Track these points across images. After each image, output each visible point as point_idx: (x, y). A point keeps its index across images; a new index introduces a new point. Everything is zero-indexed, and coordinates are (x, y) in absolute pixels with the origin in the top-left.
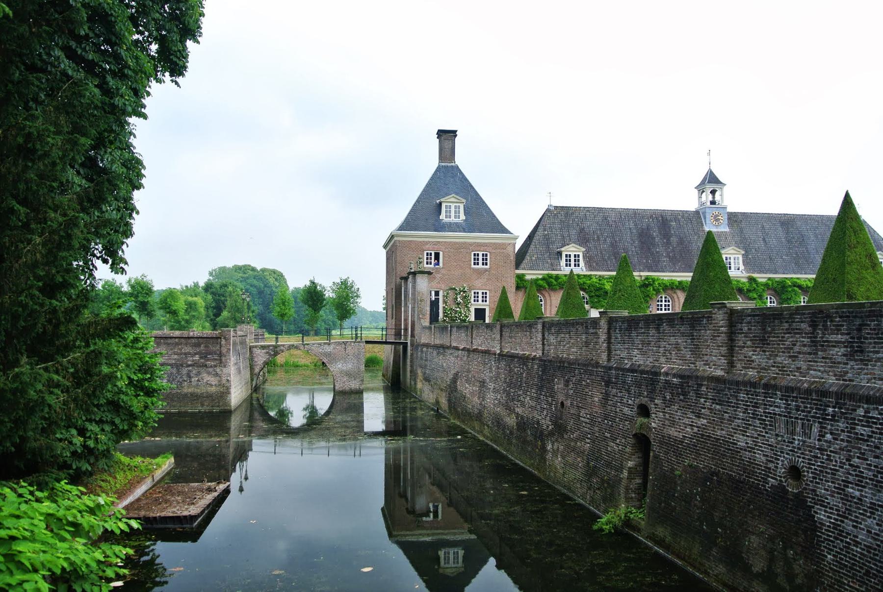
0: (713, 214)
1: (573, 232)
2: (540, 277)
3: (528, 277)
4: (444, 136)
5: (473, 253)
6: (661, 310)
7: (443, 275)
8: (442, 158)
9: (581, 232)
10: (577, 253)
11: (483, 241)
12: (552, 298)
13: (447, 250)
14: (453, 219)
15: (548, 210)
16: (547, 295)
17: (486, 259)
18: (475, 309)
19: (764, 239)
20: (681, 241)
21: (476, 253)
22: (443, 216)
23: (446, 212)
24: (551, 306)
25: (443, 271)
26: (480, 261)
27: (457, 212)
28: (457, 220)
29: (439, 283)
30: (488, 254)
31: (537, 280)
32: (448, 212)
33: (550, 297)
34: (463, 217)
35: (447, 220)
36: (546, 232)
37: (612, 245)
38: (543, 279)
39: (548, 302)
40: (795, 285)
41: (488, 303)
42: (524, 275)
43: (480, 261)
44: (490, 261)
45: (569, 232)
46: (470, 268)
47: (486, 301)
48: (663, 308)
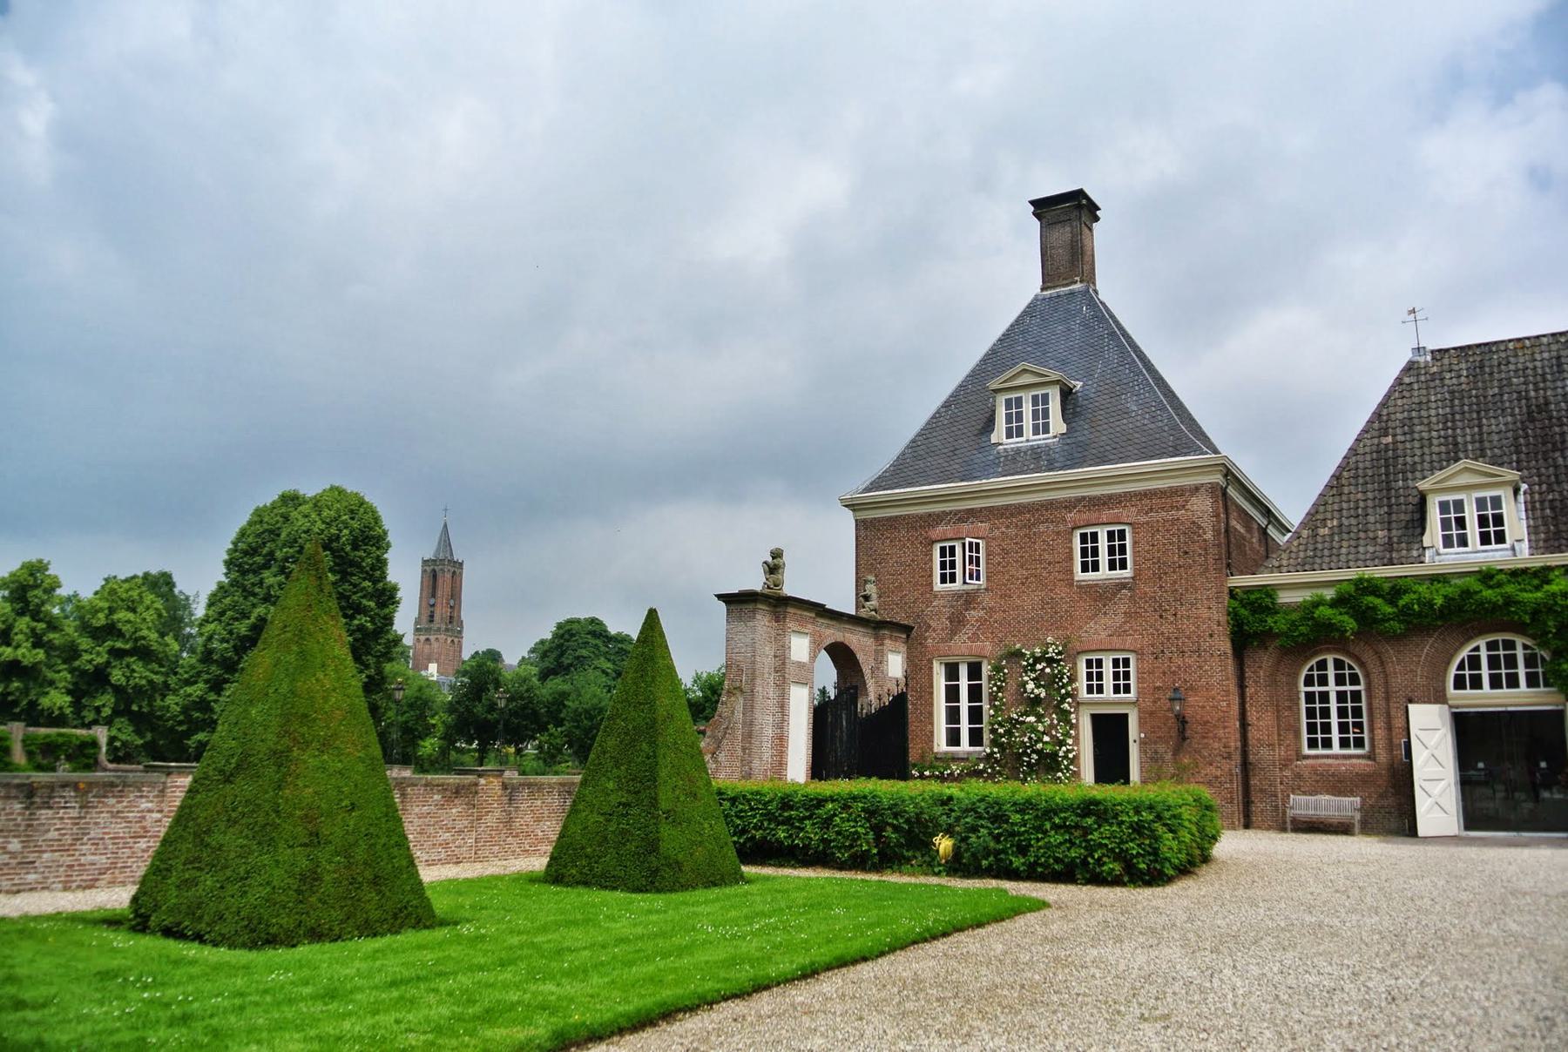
1: (1497, 425)
2: (1329, 594)
3: (1285, 598)
4: (1050, 215)
5: (1077, 534)
8: (1048, 280)
9: (1532, 420)
10: (1488, 494)
12: (1389, 668)
13: (997, 533)
14: (1029, 438)
15: (1410, 368)
16: (1369, 657)
17: (1123, 549)
21: (1089, 530)
22: (999, 434)
23: (1009, 419)
24: (1387, 699)
25: (987, 600)
26: (1104, 558)
27: (1041, 415)
28: (1041, 439)
29: (974, 638)
30: (1128, 529)
31: (1316, 604)
32: (1015, 419)
33: (1382, 663)
34: (1057, 425)
35: (1015, 442)
36: (1390, 439)
38: (1340, 602)
39: (1377, 680)
41: (1132, 695)
42: (1268, 591)
43: (1104, 558)
44: (1135, 553)
45: (1480, 426)
46: (1070, 582)
47: (1127, 689)
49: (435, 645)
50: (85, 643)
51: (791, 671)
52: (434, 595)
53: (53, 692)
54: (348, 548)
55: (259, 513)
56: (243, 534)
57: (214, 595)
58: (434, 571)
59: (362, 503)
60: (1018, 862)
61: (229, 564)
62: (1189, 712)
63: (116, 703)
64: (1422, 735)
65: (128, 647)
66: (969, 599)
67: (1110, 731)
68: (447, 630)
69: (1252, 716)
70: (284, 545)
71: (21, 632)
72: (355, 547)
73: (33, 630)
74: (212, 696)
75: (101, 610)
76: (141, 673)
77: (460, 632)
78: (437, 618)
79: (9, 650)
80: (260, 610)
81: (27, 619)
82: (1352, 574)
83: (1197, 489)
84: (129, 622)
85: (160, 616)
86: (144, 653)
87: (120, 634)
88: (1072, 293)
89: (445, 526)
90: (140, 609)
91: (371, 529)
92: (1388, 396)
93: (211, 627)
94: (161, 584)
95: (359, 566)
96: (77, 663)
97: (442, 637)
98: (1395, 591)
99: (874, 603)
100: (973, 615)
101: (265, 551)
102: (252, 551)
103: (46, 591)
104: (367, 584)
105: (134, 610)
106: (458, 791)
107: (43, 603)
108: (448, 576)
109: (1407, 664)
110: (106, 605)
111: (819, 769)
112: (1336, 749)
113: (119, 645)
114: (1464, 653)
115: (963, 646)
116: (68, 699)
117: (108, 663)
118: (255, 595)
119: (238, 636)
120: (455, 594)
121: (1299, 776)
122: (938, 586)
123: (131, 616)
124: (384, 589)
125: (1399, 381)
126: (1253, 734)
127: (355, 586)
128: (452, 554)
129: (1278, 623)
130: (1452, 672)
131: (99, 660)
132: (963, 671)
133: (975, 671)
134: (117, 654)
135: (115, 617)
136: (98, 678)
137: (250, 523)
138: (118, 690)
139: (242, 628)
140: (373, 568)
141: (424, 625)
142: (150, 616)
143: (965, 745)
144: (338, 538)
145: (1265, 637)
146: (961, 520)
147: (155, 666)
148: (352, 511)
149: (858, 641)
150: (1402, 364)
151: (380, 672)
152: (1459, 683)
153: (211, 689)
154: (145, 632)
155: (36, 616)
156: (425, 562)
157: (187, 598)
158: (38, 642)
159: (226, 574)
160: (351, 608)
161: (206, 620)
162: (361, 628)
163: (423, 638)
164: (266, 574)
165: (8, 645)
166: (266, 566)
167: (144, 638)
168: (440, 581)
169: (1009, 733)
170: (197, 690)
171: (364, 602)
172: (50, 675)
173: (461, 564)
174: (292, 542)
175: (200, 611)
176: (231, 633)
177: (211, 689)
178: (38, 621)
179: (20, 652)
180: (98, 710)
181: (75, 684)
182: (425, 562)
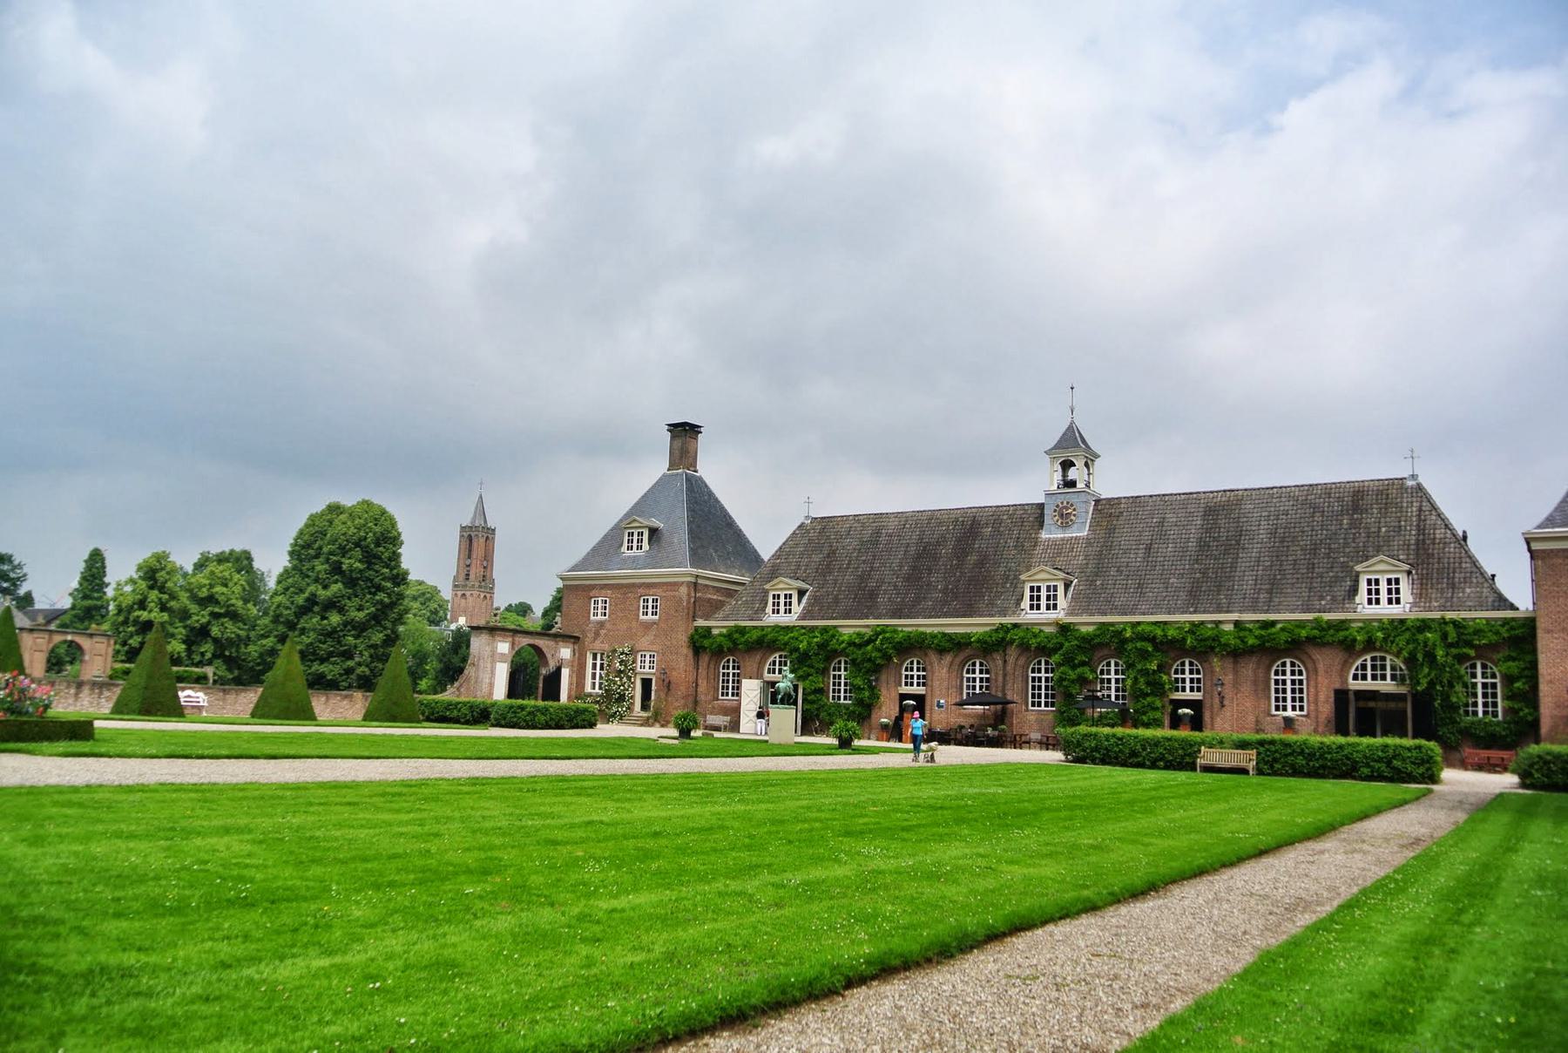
0: (1058, 506)
1: (816, 558)
2: (724, 631)
3: (715, 632)
6: (912, 684)
7: (609, 630)
8: (672, 466)
11: (676, 580)
15: (801, 526)
18: (642, 679)
19: (1149, 548)
20: (981, 563)
25: (608, 625)
29: (602, 642)
34: (646, 546)
37: (861, 577)
40: (1143, 637)
42: (709, 629)
48: (1188, 685)
49: (470, 599)
50: (193, 608)
51: (497, 657)
52: (469, 557)
53: (174, 642)
54: (373, 546)
55: (312, 518)
56: (301, 533)
57: (281, 575)
58: (470, 536)
59: (384, 512)
60: (503, 722)
61: (291, 553)
62: (671, 679)
63: (215, 651)
64: (748, 692)
65: (222, 611)
66: (601, 624)
67: (646, 684)
68: (480, 587)
69: (700, 681)
70: (329, 544)
71: (153, 601)
72: (378, 545)
73: (160, 599)
74: (279, 647)
75: (205, 585)
76: (231, 629)
77: (492, 589)
78: (472, 577)
79: (145, 613)
80: (312, 588)
81: (156, 592)
82: (732, 624)
83: (683, 583)
84: (223, 594)
85: (244, 589)
86: (233, 616)
87: (217, 602)
88: (677, 474)
89: (481, 497)
90: (230, 584)
91: (389, 532)
92: (787, 541)
93: (278, 599)
94: (242, 561)
95: (380, 558)
96: (189, 622)
97: (475, 593)
98: (742, 631)
99: (559, 625)
100: (603, 632)
101: (316, 546)
102: (308, 546)
103: (168, 573)
104: (386, 570)
105: (226, 585)
106: (346, 697)
107: (166, 582)
108: (482, 540)
109: (751, 663)
110: (208, 582)
111: (511, 694)
112: (730, 697)
113: (217, 610)
114: (771, 659)
115: (598, 645)
116: (184, 646)
117: (209, 623)
118: (308, 576)
119: (297, 606)
120: (488, 557)
121: (714, 708)
122: (592, 618)
123: (224, 590)
124: (398, 575)
125: (794, 533)
126: (700, 689)
127: (377, 572)
128: (485, 522)
129: (706, 643)
130: (767, 666)
131: (204, 621)
132: (599, 656)
133: (602, 654)
134: (215, 616)
135: (214, 590)
136: (203, 632)
137: (307, 526)
138: (216, 641)
139: (300, 600)
140: (390, 559)
141: (461, 581)
142: (237, 589)
143: (597, 690)
144: (366, 538)
145: (705, 649)
146: (602, 588)
147: (241, 625)
148: (376, 519)
149: (541, 643)
150: (799, 524)
151: (394, 632)
152: (769, 672)
153: (279, 641)
154: (233, 601)
155: (162, 589)
156: (463, 529)
157: (263, 574)
158: (163, 608)
159: (289, 561)
160: (373, 586)
161: (276, 594)
162: (381, 602)
163: (460, 593)
164: (316, 562)
165: (145, 610)
166: (317, 556)
167: (233, 605)
168: (475, 544)
169: (609, 685)
170: (269, 642)
171: (383, 583)
172: (171, 630)
173: (494, 530)
174: (333, 542)
175: (272, 583)
176: (292, 603)
177: (279, 641)
178: (165, 593)
179: (153, 615)
180: (203, 654)
181: (187, 636)
182: (463, 529)
